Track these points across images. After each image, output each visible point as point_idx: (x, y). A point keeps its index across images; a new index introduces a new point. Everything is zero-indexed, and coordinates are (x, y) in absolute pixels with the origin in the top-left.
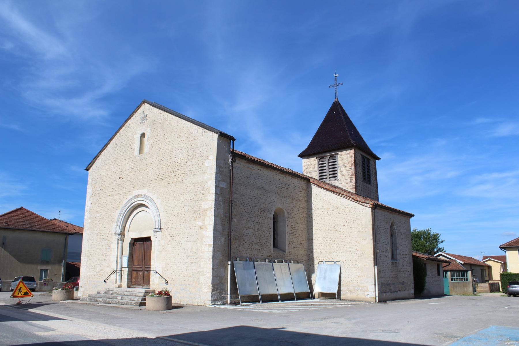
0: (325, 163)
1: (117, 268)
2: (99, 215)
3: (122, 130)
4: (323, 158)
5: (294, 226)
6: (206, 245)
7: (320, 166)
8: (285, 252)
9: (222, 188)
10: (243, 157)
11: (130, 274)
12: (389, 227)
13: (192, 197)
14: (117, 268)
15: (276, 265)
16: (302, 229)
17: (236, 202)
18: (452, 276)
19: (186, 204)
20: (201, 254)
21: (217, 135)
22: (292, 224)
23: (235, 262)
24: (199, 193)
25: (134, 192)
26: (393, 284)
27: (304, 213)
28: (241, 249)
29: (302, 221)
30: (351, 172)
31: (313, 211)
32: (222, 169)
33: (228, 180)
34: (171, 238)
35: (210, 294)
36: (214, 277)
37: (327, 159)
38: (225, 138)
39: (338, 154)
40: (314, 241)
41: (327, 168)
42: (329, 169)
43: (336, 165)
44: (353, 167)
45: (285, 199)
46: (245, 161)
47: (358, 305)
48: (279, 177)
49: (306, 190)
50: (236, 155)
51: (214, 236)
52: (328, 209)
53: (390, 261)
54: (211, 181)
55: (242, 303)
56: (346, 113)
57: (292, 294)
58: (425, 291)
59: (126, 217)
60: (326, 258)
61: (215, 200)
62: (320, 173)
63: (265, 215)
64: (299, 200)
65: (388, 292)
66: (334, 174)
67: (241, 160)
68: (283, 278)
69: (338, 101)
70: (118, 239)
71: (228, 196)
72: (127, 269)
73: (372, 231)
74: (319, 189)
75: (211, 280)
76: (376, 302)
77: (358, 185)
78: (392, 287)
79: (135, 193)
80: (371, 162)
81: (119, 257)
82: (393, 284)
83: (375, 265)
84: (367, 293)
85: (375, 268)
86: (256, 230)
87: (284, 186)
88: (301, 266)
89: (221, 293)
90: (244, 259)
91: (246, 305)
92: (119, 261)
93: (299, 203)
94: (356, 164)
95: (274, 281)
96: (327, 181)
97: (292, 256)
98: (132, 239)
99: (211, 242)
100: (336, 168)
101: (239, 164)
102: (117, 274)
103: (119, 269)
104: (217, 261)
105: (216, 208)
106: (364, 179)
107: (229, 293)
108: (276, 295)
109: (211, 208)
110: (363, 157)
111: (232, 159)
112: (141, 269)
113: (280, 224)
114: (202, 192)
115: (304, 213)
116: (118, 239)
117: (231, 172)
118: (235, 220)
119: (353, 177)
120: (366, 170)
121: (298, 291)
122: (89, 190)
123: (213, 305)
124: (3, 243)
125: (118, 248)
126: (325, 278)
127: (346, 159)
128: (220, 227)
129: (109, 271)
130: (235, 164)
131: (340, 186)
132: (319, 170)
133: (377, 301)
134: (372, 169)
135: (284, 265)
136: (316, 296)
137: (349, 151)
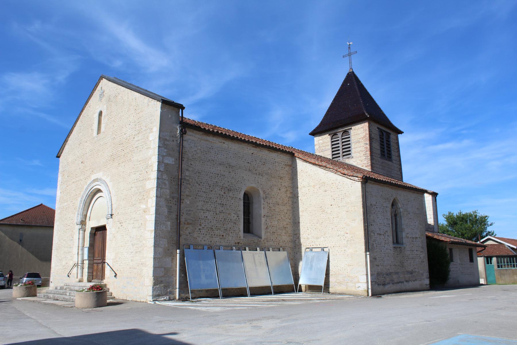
0: (338, 140)
1: (78, 261)
2: (66, 204)
3: (84, 111)
4: (335, 134)
5: (273, 208)
6: (148, 231)
7: (333, 143)
8: (261, 238)
9: (167, 165)
10: (196, 127)
11: (91, 266)
12: (390, 205)
14: (78, 261)
15: (247, 254)
16: (286, 211)
17: (188, 181)
18: (498, 263)
19: (133, 186)
20: (144, 242)
21: (161, 103)
22: (271, 205)
23: (186, 251)
25: (92, 176)
26: (397, 273)
27: (288, 192)
28: (195, 236)
29: (286, 202)
30: (366, 148)
31: (299, 189)
32: (167, 143)
33: (177, 155)
34: (119, 225)
35: (151, 288)
36: (155, 268)
37: (340, 135)
38: (170, 106)
39: (351, 129)
40: (301, 225)
41: (340, 145)
42: (343, 146)
43: (349, 141)
44: (368, 142)
45: (261, 177)
46: (201, 133)
47: (350, 299)
48: (252, 151)
49: (290, 166)
50: (187, 126)
51: (156, 220)
52: (314, 186)
53: (391, 245)
55: (193, 298)
56: (362, 84)
57: (268, 288)
58: (451, 281)
59: (87, 204)
60: (313, 244)
61: (158, 178)
62: (333, 152)
63: (230, 195)
64: (281, 178)
65: (389, 283)
66: (347, 152)
67: (195, 132)
68: (257, 267)
69: (353, 72)
70: (79, 229)
71: (177, 174)
73: (362, 210)
74: (305, 164)
75: (152, 272)
76: (368, 295)
77: (374, 162)
78: (395, 277)
79: (93, 177)
80: (392, 136)
81: (80, 248)
82: (397, 273)
83: (366, 251)
84: (358, 285)
85: (366, 255)
86: (218, 213)
87: (258, 162)
88: (283, 255)
89: (166, 287)
90: (200, 247)
91: (198, 301)
92: (80, 253)
93: (280, 181)
94: (371, 139)
95: (244, 272)
96: (341, 159)
97: (271, 243)
98: (92, 228)
99: (153, 228)
100: (350, 144)
101: (191, 136)
102: (78, 267)
103: (79, 262)
104: (160, 250)
105: (159, 186)
106: (383, 155)
107: (177, 287)
108: (245, 289)
109: (153, 188)
110: (381, 131)
111: (181, 131)
112: (100, 261)
113: (255, 206)
115: (288, 192)
116: (79, 229)
117: (181, 145)
118: (187, 202)
119: (368, 153)
120: (385, 145)
121: (277, 282)
122: (60, 179)
123: (153, 301)
124: (21, 240)
125: (79, 239)
126: (311, 268)
127: (360, 134)
128: (165, 210)
129: (71, 264)
130: (186, 137)
131: (354, 164)
132: (333, 148)
133: (370, 295)
134: (392, 144)
135: (259, 254)
136: (303, 289)
137: (363, 125)
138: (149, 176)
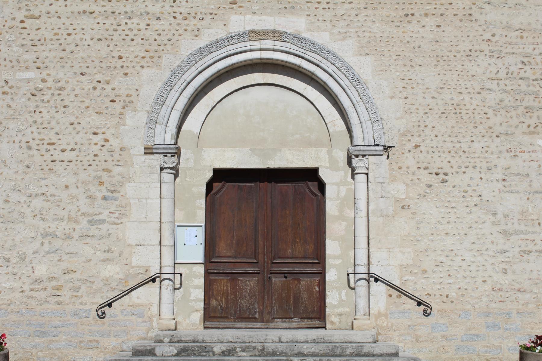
13: (512, 68)
34: (434, 180)
72: (201, 270)
79: (240, 22)
98: (216, 171)
116: (162, 169)
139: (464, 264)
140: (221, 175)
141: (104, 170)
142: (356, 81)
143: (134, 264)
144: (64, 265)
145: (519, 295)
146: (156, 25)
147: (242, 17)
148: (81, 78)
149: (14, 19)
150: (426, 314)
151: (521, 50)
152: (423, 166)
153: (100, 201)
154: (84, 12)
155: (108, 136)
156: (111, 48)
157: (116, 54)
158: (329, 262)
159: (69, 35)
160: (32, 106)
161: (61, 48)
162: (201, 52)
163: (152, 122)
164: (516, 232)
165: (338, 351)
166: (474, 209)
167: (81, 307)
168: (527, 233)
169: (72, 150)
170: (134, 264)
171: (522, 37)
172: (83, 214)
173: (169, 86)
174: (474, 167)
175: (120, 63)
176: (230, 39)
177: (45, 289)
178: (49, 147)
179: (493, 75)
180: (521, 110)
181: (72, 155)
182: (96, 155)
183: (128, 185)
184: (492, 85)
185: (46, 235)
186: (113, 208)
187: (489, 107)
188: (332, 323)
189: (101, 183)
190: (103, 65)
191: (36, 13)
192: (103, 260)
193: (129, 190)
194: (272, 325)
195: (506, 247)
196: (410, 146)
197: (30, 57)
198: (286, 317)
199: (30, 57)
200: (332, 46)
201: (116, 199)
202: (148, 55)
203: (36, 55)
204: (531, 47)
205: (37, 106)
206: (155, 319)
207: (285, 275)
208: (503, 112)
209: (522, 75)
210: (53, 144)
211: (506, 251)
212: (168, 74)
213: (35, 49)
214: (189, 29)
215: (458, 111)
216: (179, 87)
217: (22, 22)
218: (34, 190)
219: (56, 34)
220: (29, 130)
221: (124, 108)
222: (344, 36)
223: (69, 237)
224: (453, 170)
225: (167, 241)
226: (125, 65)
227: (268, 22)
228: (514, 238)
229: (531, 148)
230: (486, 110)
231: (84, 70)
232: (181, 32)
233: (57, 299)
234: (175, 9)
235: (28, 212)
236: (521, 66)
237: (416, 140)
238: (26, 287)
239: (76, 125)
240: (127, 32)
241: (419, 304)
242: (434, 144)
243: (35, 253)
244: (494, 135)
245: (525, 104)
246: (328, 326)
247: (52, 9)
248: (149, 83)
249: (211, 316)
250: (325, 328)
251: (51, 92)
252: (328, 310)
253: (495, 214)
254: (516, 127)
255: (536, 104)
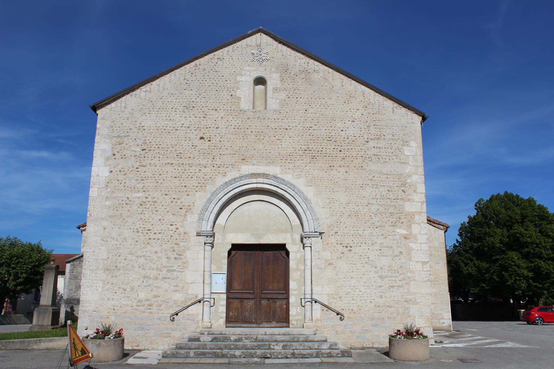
2: (140, 195)
6: (417, 262)
13: (384, 193)
20: (409, 275)
24: (396, 189)
54: (417, 176)
72: (225, 296)
79: (246, 169)
84: (442, 321)
98: (233, 245)
109: (421, 212)
114: (403, 188)
116: (205, 244)
138: (410, 197)
139: (361, 293)
140: (236, 247)
141: (176, 244)
142: (306, 199)
143: (190, 293)
144: (154, 293)
145: (389, 309)
146: (204, 170)
147: (248, 167)
148: (166, 197)
149: (133, 167)
150: (341, 319)
151: (387, 184)
152: (339, 242)
153: (173, 260)
154: (168, 163)
155: (178, 226)
156: (181, 182)
157: (184, 185)
158: (291, 292)
159: (160, 175)
160: (140, 210)
161: (156, 181)
162: (227, 184)
163: (201, 219)
164: (387, 276)
165: (296, 339)
166: (365, 265)
167: (162, 315)
168: (392, 277)
169: (160, 233)
170: (190, 293)
171: (387, 178)
172: (164, 267)
173: (210, 201)
174: (365, 243)
175: (185, 189)
176: (241, 178)
177: (144, 305)
178: (148, 232)
179: (374, 197)
180: (388, 214)
181: (159, 236)
182: (171, 236)
183: (188, 252)
184: (374, 202)
185: (145, 277)
186: (179, 264)
187: (372, 213)
188: (293, 324)
189: (174, 251)
190: (176, 190)
191: (144, 164)
192: (174, 291)
193: (188, 254)
194: (261, 326)
195: (381, 284)
196: (333, 232)
197: (141, 186)
198: (268, 321)
199: (141, 186)
200: (294, 182)
201: (181, 259)
202: (199, 185)
203: (143, 185)
204: (392, 183)
205: (143, 211)
206: (200, 322)
207: (268, 299)
208: (379, 215)
209: (388, 196)
210: (150, 230)
211: (382, 286)
212: (209, 195)
213: (143, 182)
214: (221, 172)
215: (357, 215)
216: (215, 202)
217: (137, 168)
218: (139, 253)
219: (154, 174)
220: (138, 223)
221: (186, 212)
222: (299, 177)
223: (157, 278)
224: (355, 245)
225: (207, 281)
226: (188, 190)
227: (261, 169)
228: (386, 279)
229: (393, 233)
230: (371, 214)
231: (167, 193)
232: (216, 174)
233: (150, 311)
234: (214, 162)
235: (136, 265)
236: (387, 192)
237: (336, 229)
238: (134, 304)
239: (162, 221)
240: (190, 174)
241: (338, 314)
242: (345, 231)
243: (139, 286)
244: (375, 227)
245: (390, 211)
246: (290, 326)
247: (152, 162)
248: (199, 199)
249: (230, 320)
250: (289, 327)
251: (150, 203)
252: (290, 318)
253: (376, 267)
254: (386, 223)
255: (395, 211)
